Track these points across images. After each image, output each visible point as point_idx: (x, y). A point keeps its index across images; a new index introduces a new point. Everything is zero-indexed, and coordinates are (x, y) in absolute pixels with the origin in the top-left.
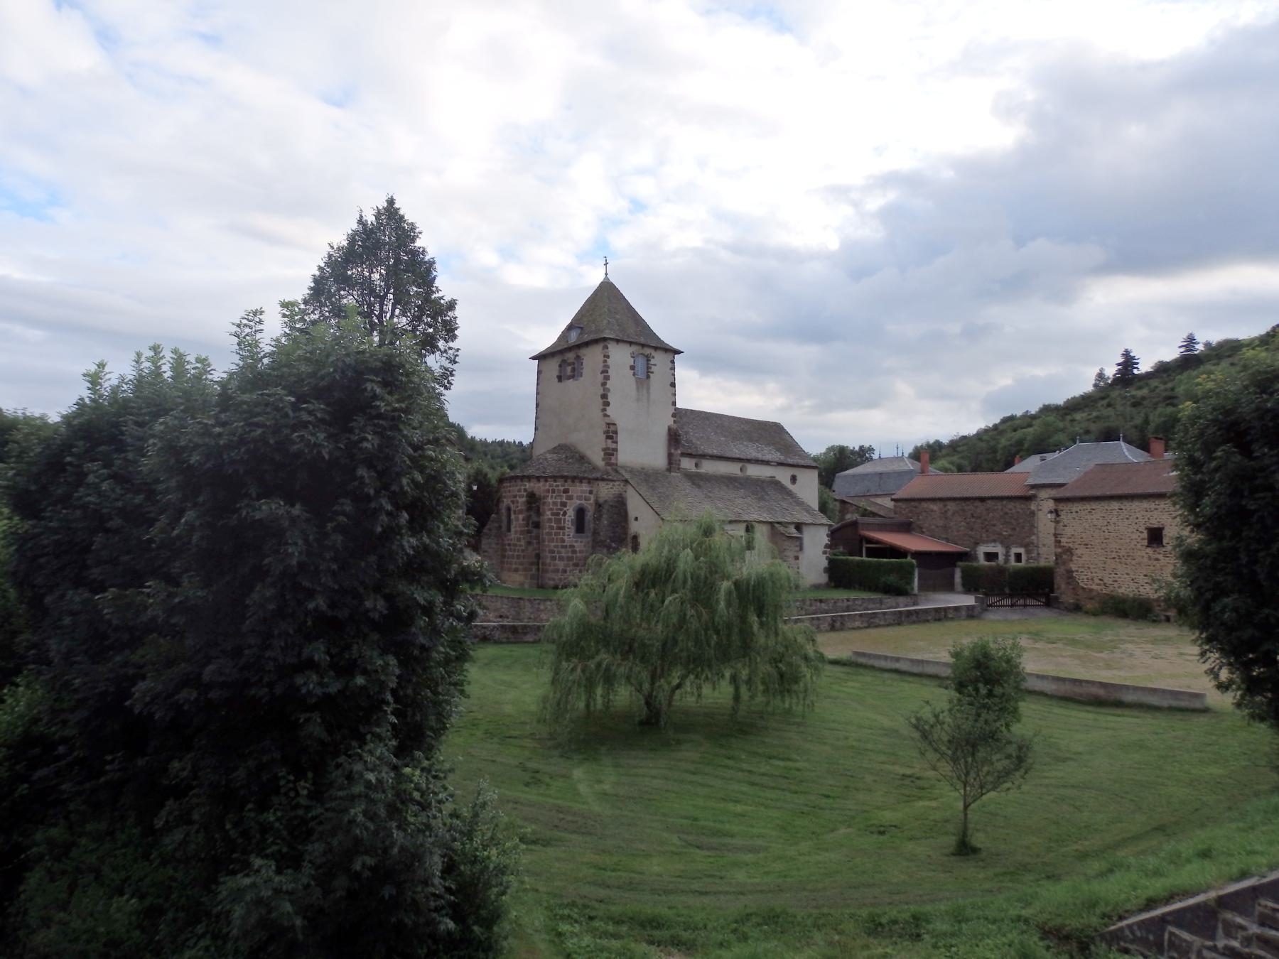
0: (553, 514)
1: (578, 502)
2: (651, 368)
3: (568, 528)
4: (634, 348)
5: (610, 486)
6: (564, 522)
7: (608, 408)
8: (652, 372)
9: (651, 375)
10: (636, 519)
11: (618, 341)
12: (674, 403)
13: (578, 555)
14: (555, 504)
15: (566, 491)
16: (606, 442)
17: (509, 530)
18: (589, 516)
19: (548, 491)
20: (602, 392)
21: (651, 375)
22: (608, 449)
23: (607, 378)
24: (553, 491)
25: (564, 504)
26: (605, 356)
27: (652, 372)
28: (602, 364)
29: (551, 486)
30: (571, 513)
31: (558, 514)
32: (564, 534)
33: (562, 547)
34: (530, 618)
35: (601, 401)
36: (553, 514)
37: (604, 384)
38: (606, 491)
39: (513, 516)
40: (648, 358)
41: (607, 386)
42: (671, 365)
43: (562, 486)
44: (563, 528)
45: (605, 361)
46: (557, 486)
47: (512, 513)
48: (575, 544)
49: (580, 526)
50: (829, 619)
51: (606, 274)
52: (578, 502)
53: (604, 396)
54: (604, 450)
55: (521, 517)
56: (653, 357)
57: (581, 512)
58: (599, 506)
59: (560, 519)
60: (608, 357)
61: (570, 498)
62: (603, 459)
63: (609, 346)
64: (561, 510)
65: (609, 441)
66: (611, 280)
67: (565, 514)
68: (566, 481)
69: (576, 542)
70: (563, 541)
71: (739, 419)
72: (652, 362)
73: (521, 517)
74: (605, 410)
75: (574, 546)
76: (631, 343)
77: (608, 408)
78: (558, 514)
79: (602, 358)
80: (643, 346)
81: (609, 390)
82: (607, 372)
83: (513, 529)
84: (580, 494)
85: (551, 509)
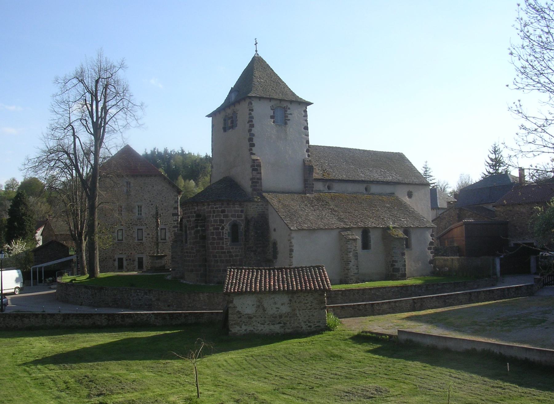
0: (214, 229)
1: (233, 219)
2: (287, 117)
3: (226, 239)
4: (273, 103)
5: (256, 206)
6: (223, 235)
7: (253, 148)
8: (289, 120)
9: (288, 122)
10: (275, 230)
11: (260, 98)
12: (308, 142)
13: (234, 258)
14: (215, 221)
15: (223, 211)
16: (252, 173)
17: (186, 242)
18: (242, 228)
19: (210, 212)
20: (248, 136)
21: (288, 122)
22: (254, 178)
23: (252, 126)
24: (214, 212)
25: (222, 221)
26: (250, 110)
27: (289, 120)
28: (248, 116)
29: (212, 208)
30: (227, 227)
31: (218, 229)
32: (223, 243)
33: (222, 253)
34: (189, 307)
35: (248, 143)
36: (214, 229)
37: (250, 130)
38: (253, 210)
39: (188, 232)
40: (285, 109)
41: (252, 132)
42: (304, 114)
43: (220, 207)
44: (222, 239)
45: (250, 114)
46: (217, 208)
47: (187, 229)
48: (231, 250)
49: (235, 238)
50: (411, 301)
51: (256, 51)
52: (233, 219)
53: (251, 140)
54: (251, 179)
55: (193, 231)
56: (289, 109)
57: (235, 227)
58: (248, 221)
59: (220, 232)
60: (252, 110)
61: (226, 216)
62: (251, 187)
63: (253, 102)
64: (220, 225)
65: (255, 173)
66: (260, 55)
67: (223, 228)
68: (222, 204)
69: (232, 248)
70: (222, 248)
71: (329, 147)
72: (289, 112)
73: (193, 231)
74: (251, 150)
75: (231, 252)
76: (270, 99)
77: (253, 148)
78: (218, 229)
79: (248, 112)
80: (281, 100)
81: (253, 135)
82: (252, 121)
83: (188, 242)
84: (233, 213)
85: (214, 225)
